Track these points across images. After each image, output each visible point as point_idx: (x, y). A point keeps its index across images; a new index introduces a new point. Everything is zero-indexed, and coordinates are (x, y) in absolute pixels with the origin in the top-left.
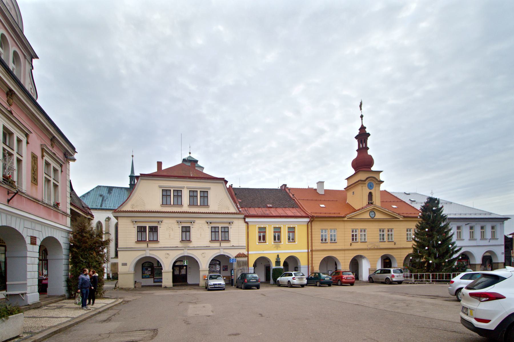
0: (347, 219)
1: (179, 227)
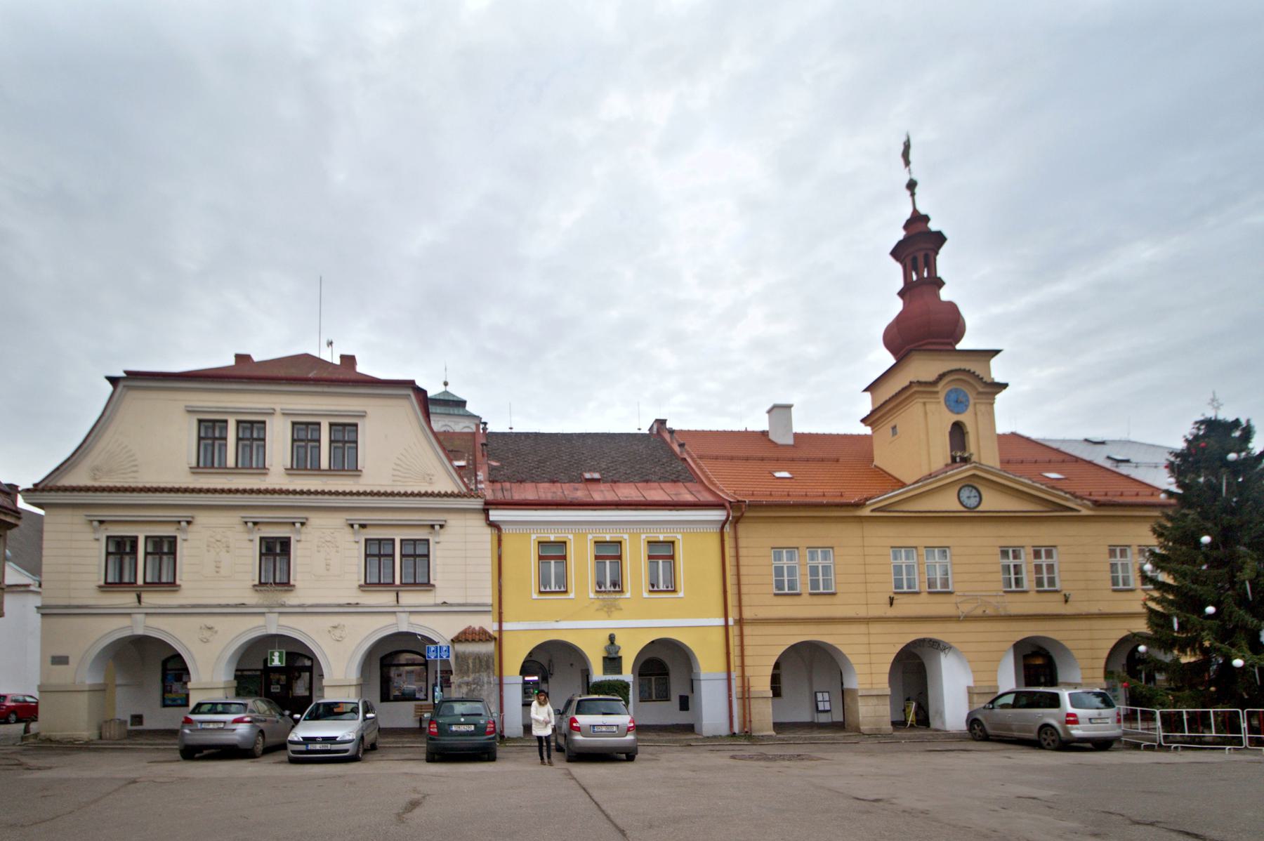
0: (873, 511)
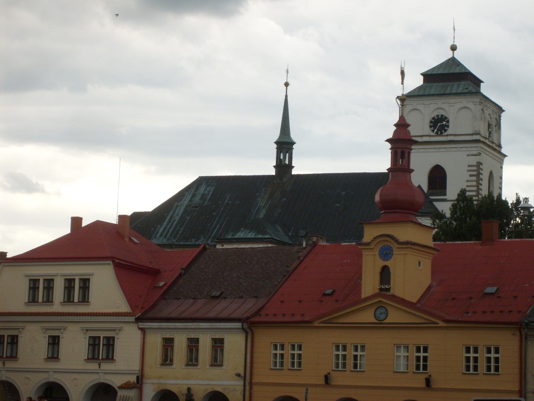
1: (45, 337)
